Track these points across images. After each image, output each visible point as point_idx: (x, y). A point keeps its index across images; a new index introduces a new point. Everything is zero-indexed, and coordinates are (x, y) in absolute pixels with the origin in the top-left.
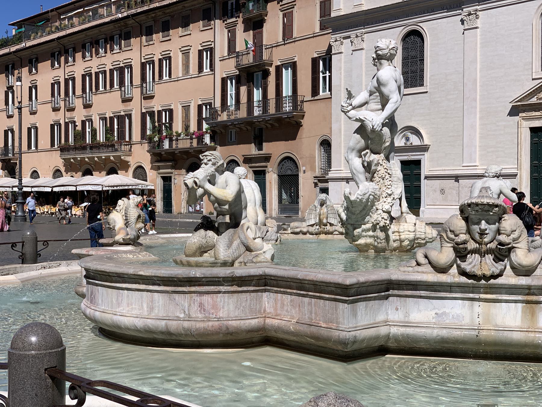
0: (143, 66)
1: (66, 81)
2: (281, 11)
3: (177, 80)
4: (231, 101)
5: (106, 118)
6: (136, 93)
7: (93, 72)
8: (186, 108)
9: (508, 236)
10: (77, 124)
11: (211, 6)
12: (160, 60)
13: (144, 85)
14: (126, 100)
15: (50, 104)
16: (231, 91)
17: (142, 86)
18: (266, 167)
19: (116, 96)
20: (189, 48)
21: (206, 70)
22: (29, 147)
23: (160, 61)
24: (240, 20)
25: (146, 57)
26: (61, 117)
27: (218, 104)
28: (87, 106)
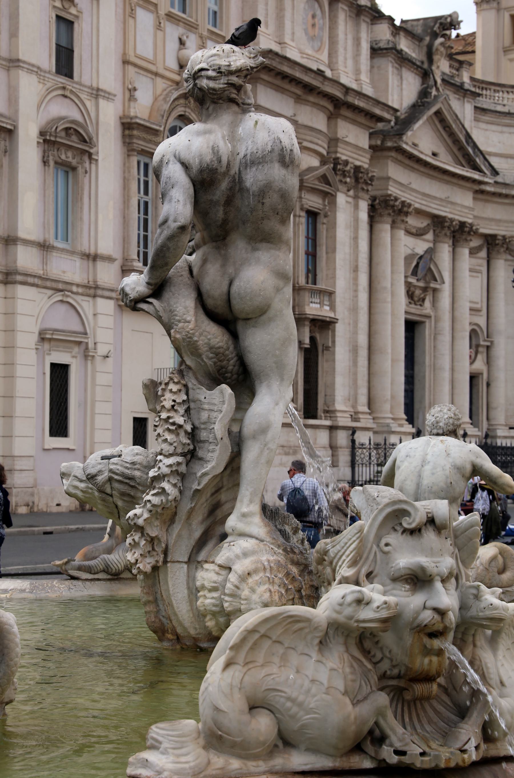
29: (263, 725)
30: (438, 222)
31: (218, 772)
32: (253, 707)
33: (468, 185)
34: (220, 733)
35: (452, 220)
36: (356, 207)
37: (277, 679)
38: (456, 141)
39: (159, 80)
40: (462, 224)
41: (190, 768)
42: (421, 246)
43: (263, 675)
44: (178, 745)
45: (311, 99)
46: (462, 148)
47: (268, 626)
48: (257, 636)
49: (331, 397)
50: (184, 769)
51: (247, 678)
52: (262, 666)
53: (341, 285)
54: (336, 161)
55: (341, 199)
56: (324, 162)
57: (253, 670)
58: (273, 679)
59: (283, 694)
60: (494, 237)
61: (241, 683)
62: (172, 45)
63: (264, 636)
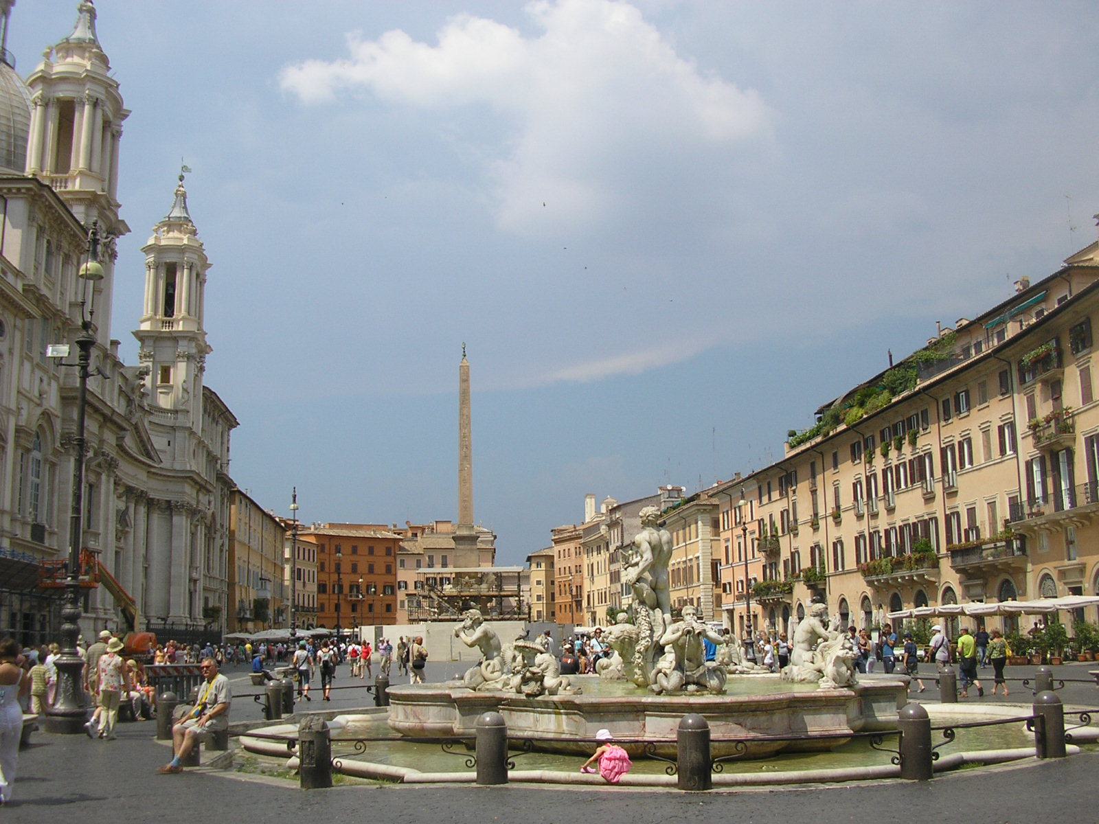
0: (943, 452)
1: (868, 479)
2: (1078, 367)
3: (979, 469)
4: (1038, 492)
5: (909, 524)
6: (938, 489)
7: (893, 466)
8: (992, 505)
9: (539, 667)
10: (881, 534)
11: (1007, 368)
12: (959, 442)
13: (946, 478)
14: (929, 498)
15: (852, 511)
16: (1037, 478)
17: (943, 480)
18: (1081, 582)
19: (917, 494)
20: (988, 424)
21: (1009, 452)
22: (836, 567)
23: (961, 444)
24: (1039, 386)
25: (946, 440)
26: (864, 527)
27: (1025, 498)
28: (891, 511)
30: (129, 490)
33: (144, 467)
35: (137, 489)
36: (108, 481)
38: (142, 441)
39: (32, 403)
40: (142, 491)
42: (122, 506)
45: (95, 416)
46: (144, 445)
49: (95, 601)
53: (101, 530)
54: (103, 454)
55: (104, 477)
56: (96, 454)
60: (152, 499)
62: (37, 382)
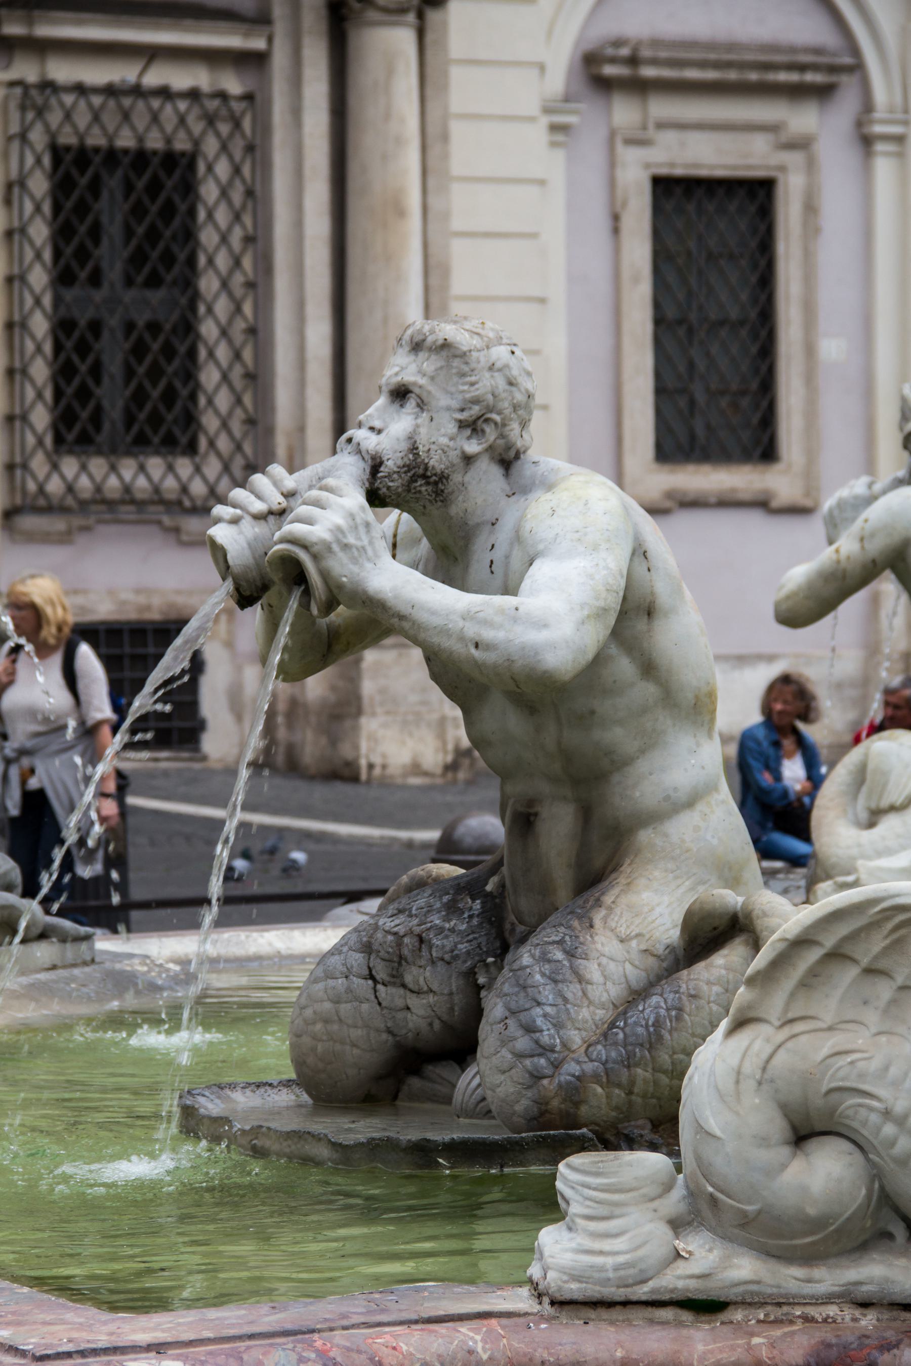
29: (824, 1176)
31: (692, 1284)
32: (803, 1133)
34: (710, 1189)
37: (861, 1065)
41: (617, 1268)
43: (825, 1051)
44: (603, 1211)
47: (843, 930)
48: (813, 955)
50: (602, 1269)
51: (781, 1057)
52: (830, 1029)
57: (803, 1039)
58: (852, 1063)
59: (875, 1103)
61: (764, 1069)
63: (836, 956)
